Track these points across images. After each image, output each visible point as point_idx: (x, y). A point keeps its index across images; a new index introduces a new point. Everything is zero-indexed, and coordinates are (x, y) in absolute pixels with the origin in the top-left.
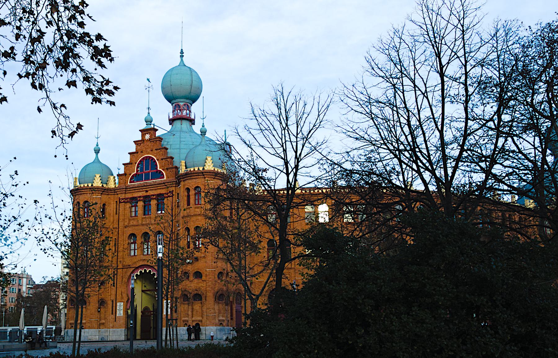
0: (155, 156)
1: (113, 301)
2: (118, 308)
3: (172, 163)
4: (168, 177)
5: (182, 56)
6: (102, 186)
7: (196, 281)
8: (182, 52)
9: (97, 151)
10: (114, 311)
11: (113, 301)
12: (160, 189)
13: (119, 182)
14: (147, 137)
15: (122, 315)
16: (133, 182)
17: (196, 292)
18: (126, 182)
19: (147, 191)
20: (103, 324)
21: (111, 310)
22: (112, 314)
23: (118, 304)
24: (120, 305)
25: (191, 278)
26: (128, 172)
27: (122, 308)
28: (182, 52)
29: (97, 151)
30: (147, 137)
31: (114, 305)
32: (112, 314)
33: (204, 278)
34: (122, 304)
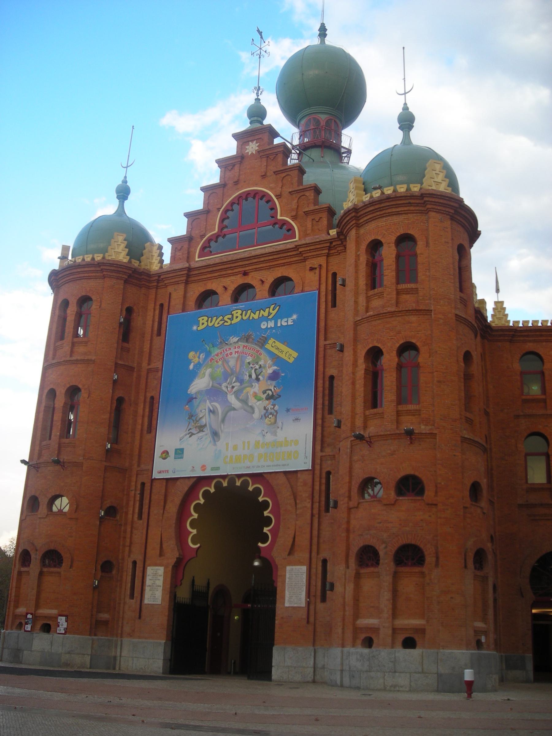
0: (271, 189)
2: (148, 582)
6: (130, 262)
9: (123, 193)
10: (137, 588)
11: (135, 563)
12: (284, 265)
13: (173, 258)
14: (252, 148)
15: (159, 602)
16: (210, 253)
18: (189, 258)
19: (245, 274)
20: (106, 623)
21: (129, 585)
22: (132, 596)
23: (150, 570)
24: (155, 574)
27: (160, 582)
29: (123, 193)
31: (139, 573)
32: (132, 596)
33: (429, 493)
34: (161, 570)
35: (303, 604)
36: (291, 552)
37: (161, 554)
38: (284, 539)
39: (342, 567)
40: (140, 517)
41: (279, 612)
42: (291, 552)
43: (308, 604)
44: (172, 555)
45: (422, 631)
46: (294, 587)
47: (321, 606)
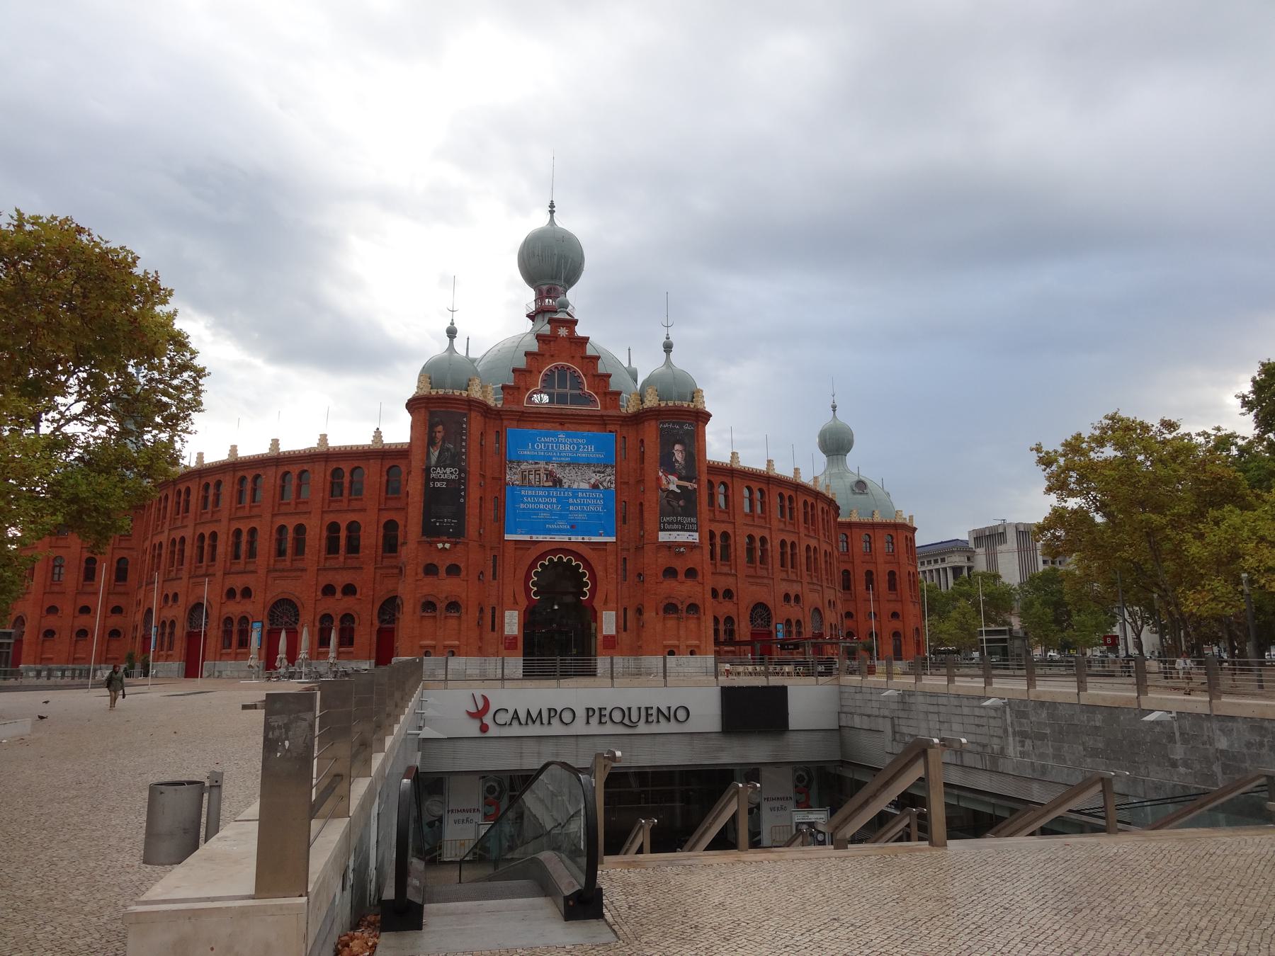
1: (494, 608)
3: (607, 385)
4: (605, 407)
5: (552, 212)
7: (689, 582)
8: (552, 206)
10: (496, 624)
11: (494, 608)
17: (691, 601)
18: (520, 402)
22: (493, 629)
23: (507, 613)
25: (681, 577)
26: (522, 384)
27: (516, 620)
28: (552, 206)
30: (563, 332)
32: (493, 629)
33: (700, 578)
35: (614, 633)
36: (606, 602)
37: (516, 602)
38: (600, 595)
39: (653, 614)
40: (494, 578)
41: (600, 637)
42: (606, 602)
43: (617, 632)
44: (523, 603)
45: (698, 647)
46: (608, 623)
47: (624, 635)
